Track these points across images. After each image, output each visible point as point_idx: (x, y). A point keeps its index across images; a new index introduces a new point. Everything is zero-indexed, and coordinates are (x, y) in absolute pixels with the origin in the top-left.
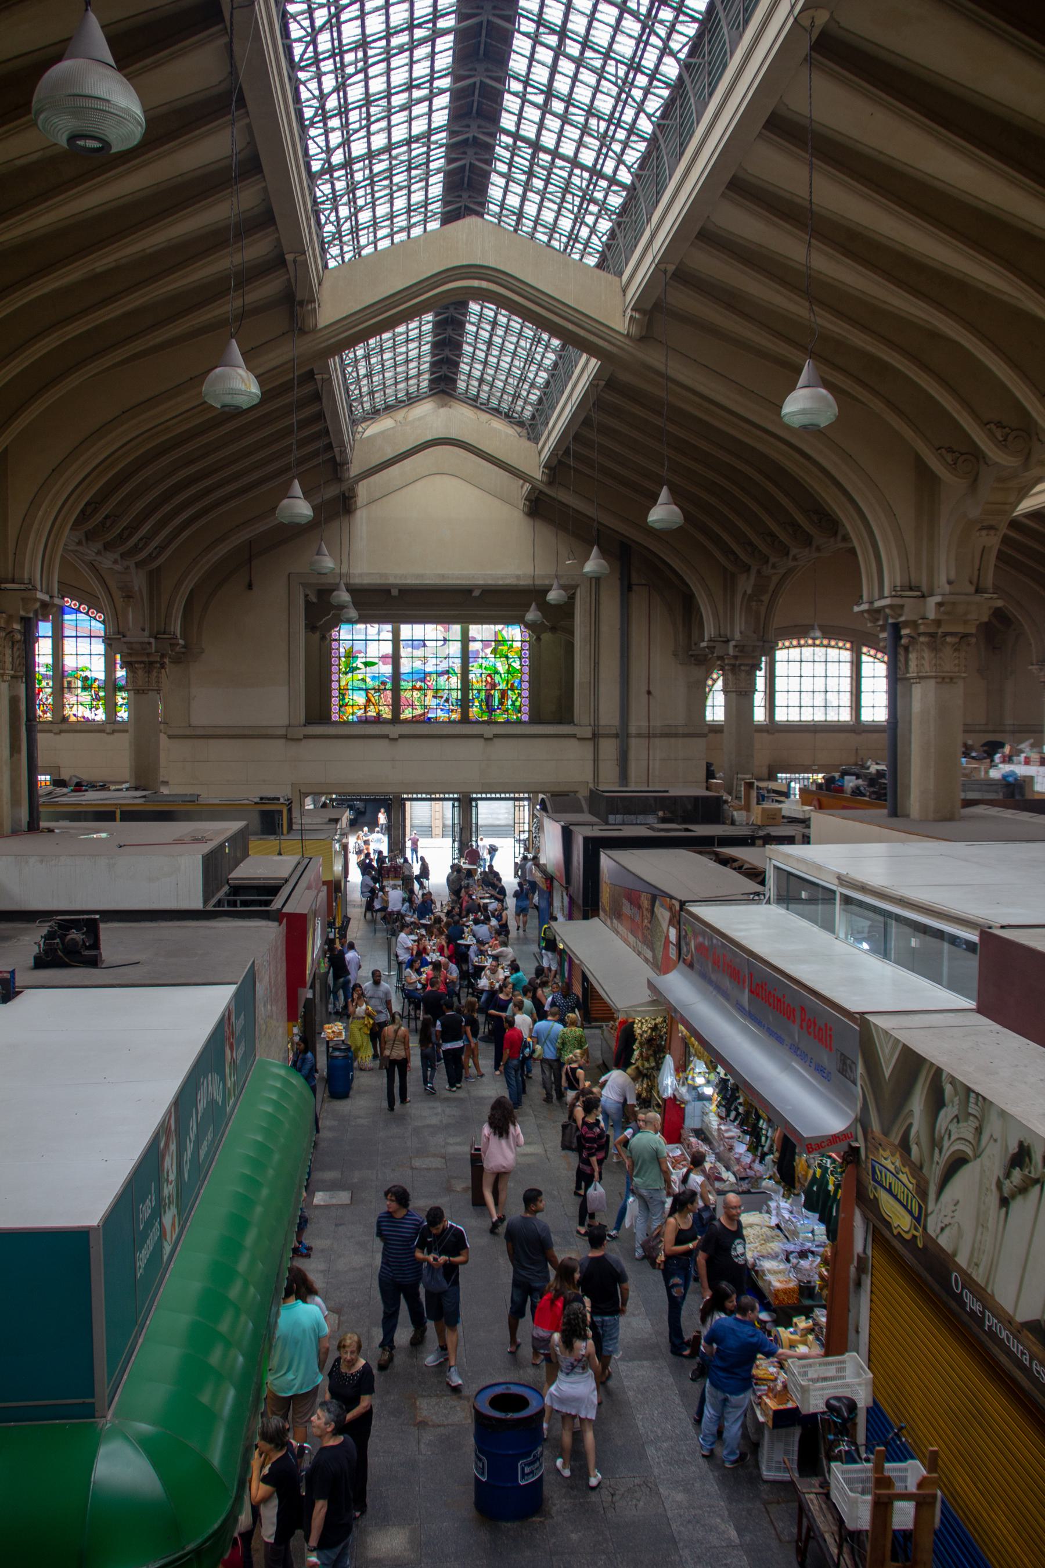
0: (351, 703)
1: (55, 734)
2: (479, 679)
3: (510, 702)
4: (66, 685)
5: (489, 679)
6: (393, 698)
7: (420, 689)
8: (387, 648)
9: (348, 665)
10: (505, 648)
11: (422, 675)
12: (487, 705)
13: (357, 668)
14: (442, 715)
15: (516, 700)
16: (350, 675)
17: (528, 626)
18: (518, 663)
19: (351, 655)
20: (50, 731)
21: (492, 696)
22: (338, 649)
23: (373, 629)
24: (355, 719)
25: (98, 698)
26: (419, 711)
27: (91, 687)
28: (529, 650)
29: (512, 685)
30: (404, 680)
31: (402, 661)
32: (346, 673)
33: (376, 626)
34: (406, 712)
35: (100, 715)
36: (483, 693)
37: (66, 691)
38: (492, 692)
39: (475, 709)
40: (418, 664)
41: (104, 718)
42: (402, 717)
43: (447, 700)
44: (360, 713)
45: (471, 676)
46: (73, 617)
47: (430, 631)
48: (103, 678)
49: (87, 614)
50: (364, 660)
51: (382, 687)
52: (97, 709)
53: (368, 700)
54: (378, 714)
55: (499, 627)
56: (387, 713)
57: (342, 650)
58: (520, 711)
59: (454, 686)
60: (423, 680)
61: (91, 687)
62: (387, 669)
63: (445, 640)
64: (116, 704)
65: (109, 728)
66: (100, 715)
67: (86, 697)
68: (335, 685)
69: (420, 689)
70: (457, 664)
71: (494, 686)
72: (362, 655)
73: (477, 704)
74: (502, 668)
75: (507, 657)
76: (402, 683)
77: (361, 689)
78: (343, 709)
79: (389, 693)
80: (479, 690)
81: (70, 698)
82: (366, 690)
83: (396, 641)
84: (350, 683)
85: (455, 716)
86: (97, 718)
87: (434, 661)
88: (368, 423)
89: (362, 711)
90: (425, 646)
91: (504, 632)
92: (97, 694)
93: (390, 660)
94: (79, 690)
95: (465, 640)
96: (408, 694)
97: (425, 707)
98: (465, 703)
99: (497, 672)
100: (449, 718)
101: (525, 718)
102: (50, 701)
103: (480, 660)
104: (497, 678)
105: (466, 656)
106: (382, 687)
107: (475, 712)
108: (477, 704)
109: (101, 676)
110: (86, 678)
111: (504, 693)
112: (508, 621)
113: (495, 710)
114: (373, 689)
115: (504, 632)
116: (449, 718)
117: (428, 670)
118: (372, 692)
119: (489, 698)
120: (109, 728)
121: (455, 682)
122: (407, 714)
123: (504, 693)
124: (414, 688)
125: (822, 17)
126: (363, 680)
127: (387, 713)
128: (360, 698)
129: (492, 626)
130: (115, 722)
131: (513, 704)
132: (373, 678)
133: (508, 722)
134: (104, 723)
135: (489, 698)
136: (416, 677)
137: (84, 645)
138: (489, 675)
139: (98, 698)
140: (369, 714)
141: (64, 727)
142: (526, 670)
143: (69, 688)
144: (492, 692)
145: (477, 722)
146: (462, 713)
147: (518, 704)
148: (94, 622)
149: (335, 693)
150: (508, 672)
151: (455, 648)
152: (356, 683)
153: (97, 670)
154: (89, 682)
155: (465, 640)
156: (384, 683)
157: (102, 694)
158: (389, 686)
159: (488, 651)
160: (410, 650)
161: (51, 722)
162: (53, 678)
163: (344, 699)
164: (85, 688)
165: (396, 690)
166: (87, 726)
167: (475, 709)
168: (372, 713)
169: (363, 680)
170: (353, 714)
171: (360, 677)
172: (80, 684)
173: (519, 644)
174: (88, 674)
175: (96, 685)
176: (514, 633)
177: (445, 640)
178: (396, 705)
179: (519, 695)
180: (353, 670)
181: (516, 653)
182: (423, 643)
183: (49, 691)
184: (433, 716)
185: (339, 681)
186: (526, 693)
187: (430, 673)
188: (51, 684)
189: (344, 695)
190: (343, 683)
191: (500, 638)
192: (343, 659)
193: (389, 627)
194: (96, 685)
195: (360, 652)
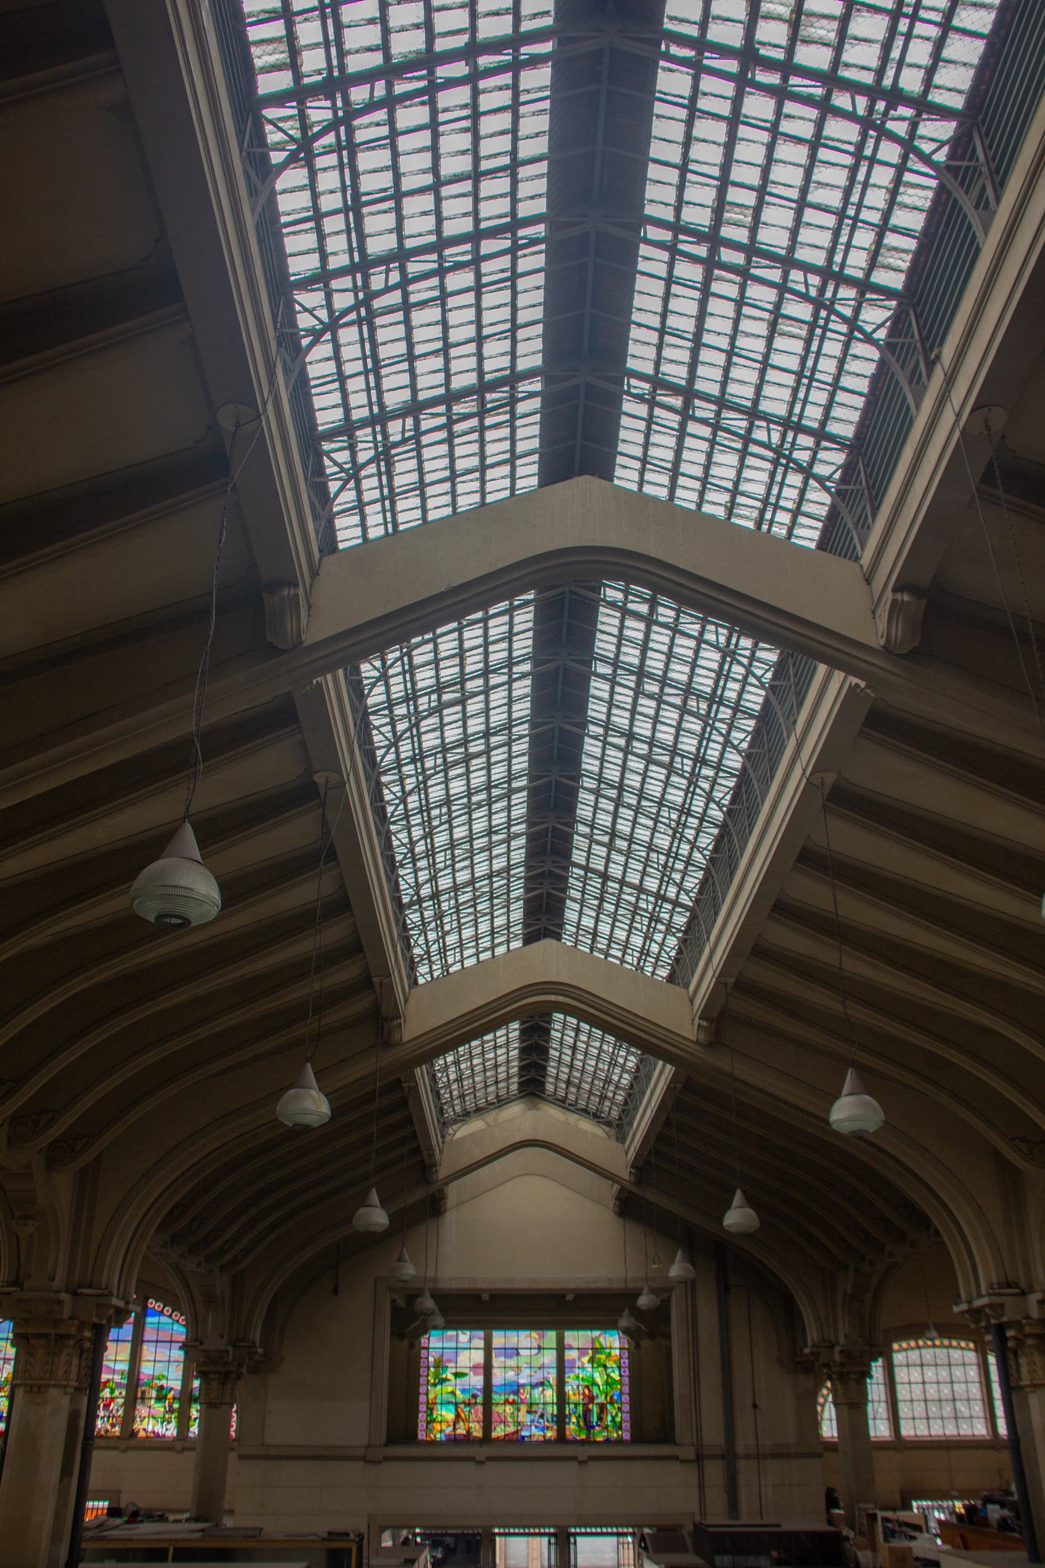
0: (439, 1419)
1: (121, 1451)
2: (576, 1392)
3: (609, 1418)
4: (139, 1395)
5: (587, 1391)
7: (513, 1403)
8: (478, 1357)
9: (437, 1375)
10: (603, 1357)
11: (516, 1388)
12: (585, 1421)
13: (446, 1380)
14: (537, 1434)
15: (616, 1414)
16: (439, 1387)
17: (626, 1331)
18: (617, 1372)
19: (440, 1365)
20: (116, 1448)
22: (427, 1358)
23: (464, 1337)
24: (443, 1438)
25: (171, 1410)
26: (511, 1429)
27: (165, 1397)
28: (629, 1358)
29: (612, 1397)
30: (496, 1393)
32: (435, 1385)
33: (468, 1333)
34: (498, 1429)
35: (170, 1430)
36: (580, 1408)
37: (139, 1401)
38: (590, 1406)
40: (511, 1374)
41: (175, 1434)
42: (494, 1435)
43: (542, 1416)
44: (449, 1430)
45: (568, 1388)
46: (155, 1320)
47: (524, 1338)
48: (179, 1388)
49: (170, 1316)
50: (454, 1370)
52: (169, 1423)
53: (458, 1416)
54: (468, 1431)
55: (596, 1333)
56: (477, 1431)
57: (431, 1359)
58: (620, 1428)
59: (549, 1400)
60: (517, 1393)
61: (165, 1397)
62: (477, 1381)
64: (190, 1418)
66: (170, 1430)
67: (159, 1408)
68: (422, 1398)
69: (513, 1403)
70: (552, 1376)
71: (591, 1399)
72: (453, 1364)
73: (574, 1419)
74: (599, 1379)
75: (605, 1367)
77: (449, 1403)
78: (430, 1426)
79: (480, 1408)
80: (576, 1405)
81: (142, 1410)
82: (456, 1404)
83: (488, 1349)
84: (439, 1397)
85: (549, 1434)
86: (168, 1433)
87: (527, 1372)
88: (459, 1125)
89: (451, 1428)
90: (518, 1354)
91: (601, 1339)
92: (171, 1406)
93: (482, 1371)
94: (153, 1401)
95: (561, 1348)
96: (499, 1409)
97: (519, 1423)
98: (561, 1419)
99: (594, 1383)
100: (544, 1436)
101: (627, 1436)
102: (121, 1412)
103: (577, 1370)
104: (595, 1390)
105: (562, 1367)
106: (473, 1401)
107: (572, 1428)
108: (574, 1419)
109: (177, 1385)
110: (162, 1388)
111: (602, 1407)
113: (593, 1427)
116: (544, 1436)
117: (522, 1381)
119: (587, 1412)
120: (179, 1445)
121: (550, 1395)
122: (498, 1432)
123: (602, 1407)
124: (507, 1402)
125: (831, 778)
126: (453, 1393)
127: (477, 1431)
128: (449, 1414)
129: (589, 1333)
131: (613, 1420)
132: (463, 1391)
133: (608, 1441)
134: (175, 1440)
135: (587, 1412)
137: (163, 1353)
138: (587, 1387)
139: (171, 1410)
140: (459, 1431)
141: (132, 1443)
142: (626, 1380)
143: (143, 1398)
144: (590, 1406)
145: (575, 1442)
148: (176, 1326)
149: (423, 1407)
150: (607, 1383)
151: (549, 1357)
153: (174, 1382)
154: (164, 1392)
155: (561, 1348)
156: (475, 1396)
157: (176, 1406)
158: (480, 1400)
159: (585, 1359)
160: (502, 1359)
161: (118, 1438)
162: (128, 1387)
163: (432, 1414)
164: (160, 1398)
165: (488, 1404)
166: (156, 1443)
167: (572, 1426)
168: (461, 1431)
169: (453, 1393)
170: (441, 1431)
171: (450, 1389)
172: (154, 1394)
173: (617, 1352)
174: (164, 1382)
175: (170, 1395)
176: (613, 1341)
177: (539, 1348)
179: (620, 1409)
180: (443, 1381)
181: (615, 1362)
182: (516, 1351)
183: (121, 1401)
185: (427, 1394)
186: (626, 1408)
187: (523, 1385)
188: (124, 1393)
189: (432, 1410)
190: (431, 1396)
191: (597, 1346)
192: (432, 1369)
193: (481, 1333)
194: (170, 1395)
195: (450, 1361)
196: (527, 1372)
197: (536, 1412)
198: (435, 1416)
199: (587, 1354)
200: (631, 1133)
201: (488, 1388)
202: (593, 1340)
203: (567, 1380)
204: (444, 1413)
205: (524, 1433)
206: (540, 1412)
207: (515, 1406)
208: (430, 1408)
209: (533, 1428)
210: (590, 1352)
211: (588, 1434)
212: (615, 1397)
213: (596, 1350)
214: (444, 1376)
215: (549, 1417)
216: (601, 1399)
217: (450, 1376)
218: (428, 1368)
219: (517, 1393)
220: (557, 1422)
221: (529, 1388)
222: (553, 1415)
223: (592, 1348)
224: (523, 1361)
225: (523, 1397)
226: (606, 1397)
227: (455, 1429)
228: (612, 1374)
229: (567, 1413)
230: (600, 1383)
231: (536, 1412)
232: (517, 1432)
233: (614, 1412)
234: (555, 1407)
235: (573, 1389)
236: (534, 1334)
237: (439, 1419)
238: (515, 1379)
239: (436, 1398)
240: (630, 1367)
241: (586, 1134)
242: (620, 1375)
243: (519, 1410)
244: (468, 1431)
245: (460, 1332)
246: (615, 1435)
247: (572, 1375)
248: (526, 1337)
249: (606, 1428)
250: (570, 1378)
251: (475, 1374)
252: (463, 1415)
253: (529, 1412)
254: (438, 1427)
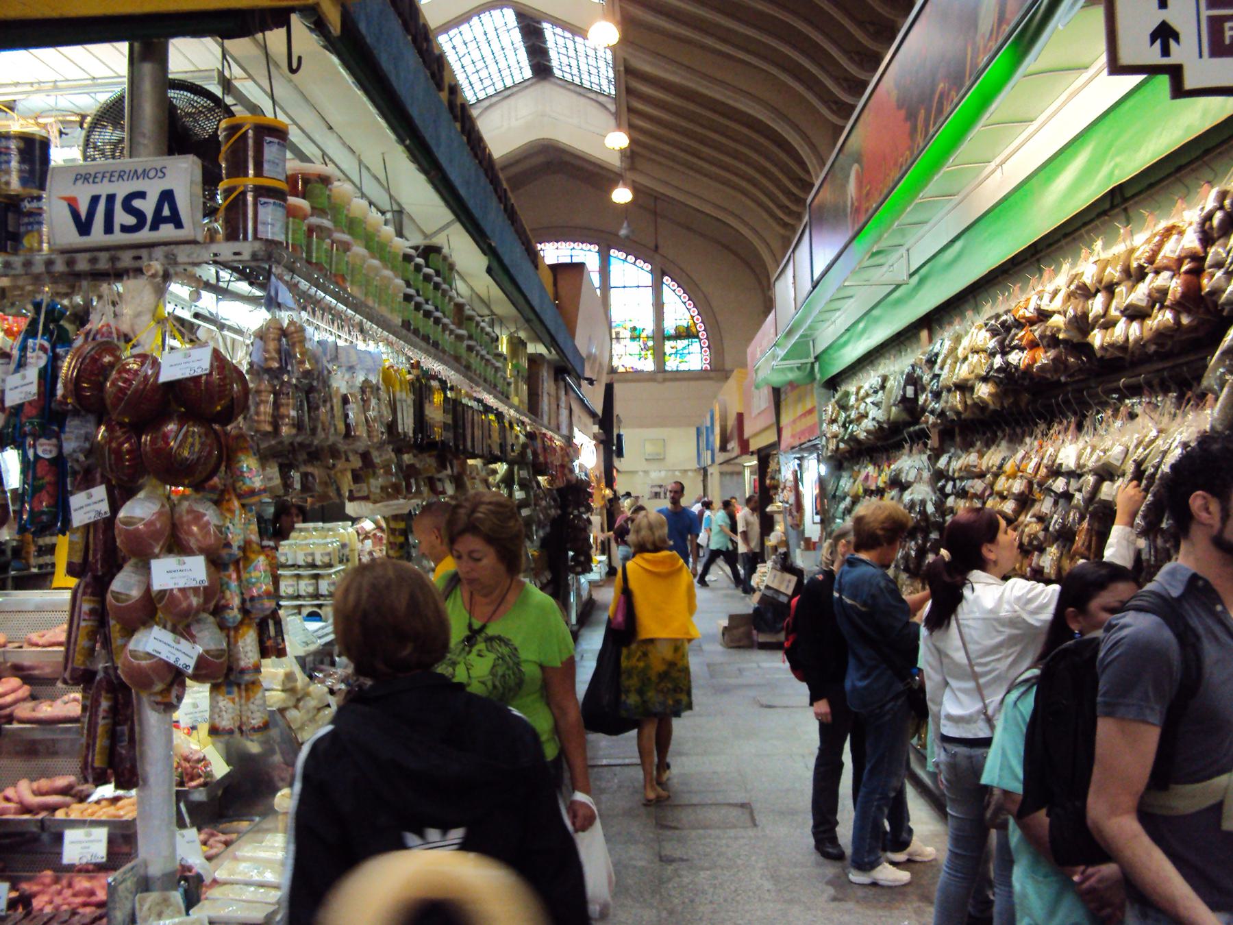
27: (639, 337)
35: (648, 365)
37: (614, 342)
49: (634, 264)
61: (639, 337)
65: (660, 376)
67: (635, 347)
92: (645, 344)
110: (634, 329)
130: (665, 371)
139: (646, 348)
143: (618, 338)
157: (650, 343)
164: (633, 338)
172: (627, 334)
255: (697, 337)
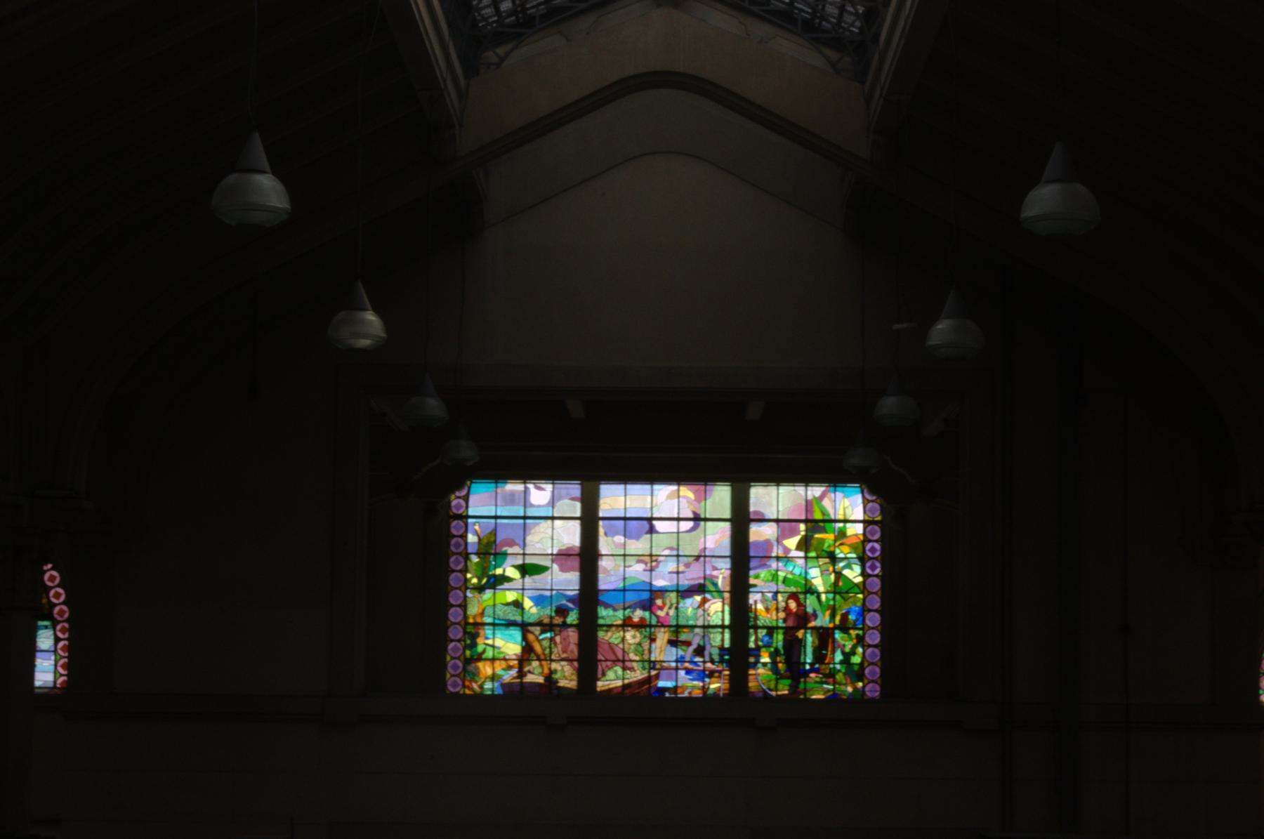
0: (489, 654)
2: (772, 605)
3: (839, 657)
5: (793, 605)
6: (581, 645)
7: (641, 625)
8: (570, 535)
9: (484, 570)
10: (829, 537)
11: (646, 596)
12: (788, 662)
13: (504, 579)
14: (689, 685)
15: (853, 653)
16: (488, 594)
17: (871, 483)
18: (857, 569)
19: (491, 550)
21: (800, 643)
22: (464, 537)
23: (540, 495)
24: (499, 691)
26: (638, 674)
28: (882, 541)
29: (845, 617)
30: (607, 606)
31: (604, 563)
32: (480, 589)
33: (548, 487)
34: (610, 675)
36: (779, 638)
38: (800, 634)
39: (761, 671)
40: (637, 571)
42: (601, 685)
43: (700, 651)
44: (509, 676)
45: (752, 598)
47: (665, 499)
50: (519, 561)
51: (558, 620)
53: (528, 649)
54: (549, 678)
55: (816, 491)
56: (567, 677)
57: (472, 538)
58: (860, 675)
59: (715, 620)
60: (648, 605)
62: (568, 580)
63: (697, 519)
68: (454, 615)
69: (641, 625)
70: (722, 573)
71: (802, 619)
72: (516, 549)
73: (765, 659)
74: (818, 580)
75: (833, 558)
76: (602, 612)
77: (510, 624)
78: (471, 668)
79: (573, 635)
80: (771, 630)
82: (524, 627)
83: (590, 521)
84: (489, 611)
87: (671, 565)
88: (509, 46)
89: (514, 672)
90: (652, 530)
91: (826, 503)
93: (576, 562)
95: (741, 519)
96: (613, 637)
97: (653, 664)
98: (738, 658)
99: (810, 590)
100: (705, 689)
101: (873, 691)
103: (774, 564)
105: (742, 556)
106: (558, 620)
107: (761, 675)
108: (765, 659)
111: (825, 636)
112: (835, 477)
113: (805, 674)
114: (539, 623)
115: (826, 503)
116: (705, 689)
117: (659, 583)
118: (537, 630)
119: (793, 646)
121: (718, 611)
122: (612, 679)
123: (825, 636)
124: (627, 624)
126: (517, 604)
127: (567, 677)
128: (510, 644)
129: (800, 489)
131: (846, 660)
132: (538, 601)
133: (834, 698)
135: (793, 646)
136: (631, 598)
138: (793, 596)
140: (529, 678)
142: (876, 584)
144: (800, 634)
146: (732, 679)
147: (856, 659)
149: (455, 633)
150: (835, 589)
151: (718, 537)
152: (501, 612)
155: (741, 519)
156: (562, 611)
158: (573, 618)
159: (791, 543)
160: (620, 539)
163: (474, 645)
165: (589, 627)
167: (761, 671)
168: (535, 676)
169: (517, 604)
170: (493, 678)
171: (511, 596)
173: (858, 529)
176: (849, 506)
177: (697, 519)
178: (589, 659)
179: (860, 640)
180: (497, 582)
181: (854, 548)
182: (649, 524)
184: (669, 684)
185: (464, 606)
186: (874, 638)
187: (662, 592)
189: (474, 637)
190: (473, 610)
191: (818, 516)
192: (475, 559)
193: (575, 488)
195: (511, 543)
196: (671, 565)
197: (688, 644)
198: (480, 648)
199: (793, 533)
200: (877, 56)
201: (589, 595)
202: (809, 505)
203: (752, 581)
204: (499, 643)
205: (661, 684)
206: (696, 641)
207: (646, 632)
208: (472, 631)
209: (682, 673)
210: (802, 527)
211: (794, 687)
212: (851, 617)
213: (815, 525)
214: (499, 571)
215: (715, 652)
216: (823, 620)
217: (512, 573)
218: (466, 557)
219: (648, 605)
220: (728, 662)
221: (673, 595)
222: (722, 648)
223: (806, 521)
224: (661, 544)
225: (661, 613)
226: (833, 616)
227: (521, 674)
228: (846, 572)
229: (752, 645)
230: (821, 589)
231: (688, 644)
232: (649, 680)
233: (849, 646)
234: (727, 635)
235: (764, 601)
236: (687, 492)
237: (489, 654)
238: (645, 577)
239: (482, 614)
240: (884, 559)
241: (783, 65)
242: (863, 574)
243: (653, 640)
244: (549, 678)
245: (531, 486)
246: (850, 689)
247: (763, 573)
248: (669, 497)
249: (831, 675)
250: (759, 578)
251: (563, 569)
252: (538, 648)
253: (673, 643)
254: (486, 669)
255: (49, 617)
